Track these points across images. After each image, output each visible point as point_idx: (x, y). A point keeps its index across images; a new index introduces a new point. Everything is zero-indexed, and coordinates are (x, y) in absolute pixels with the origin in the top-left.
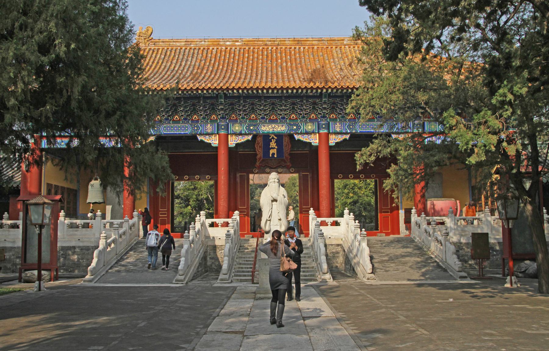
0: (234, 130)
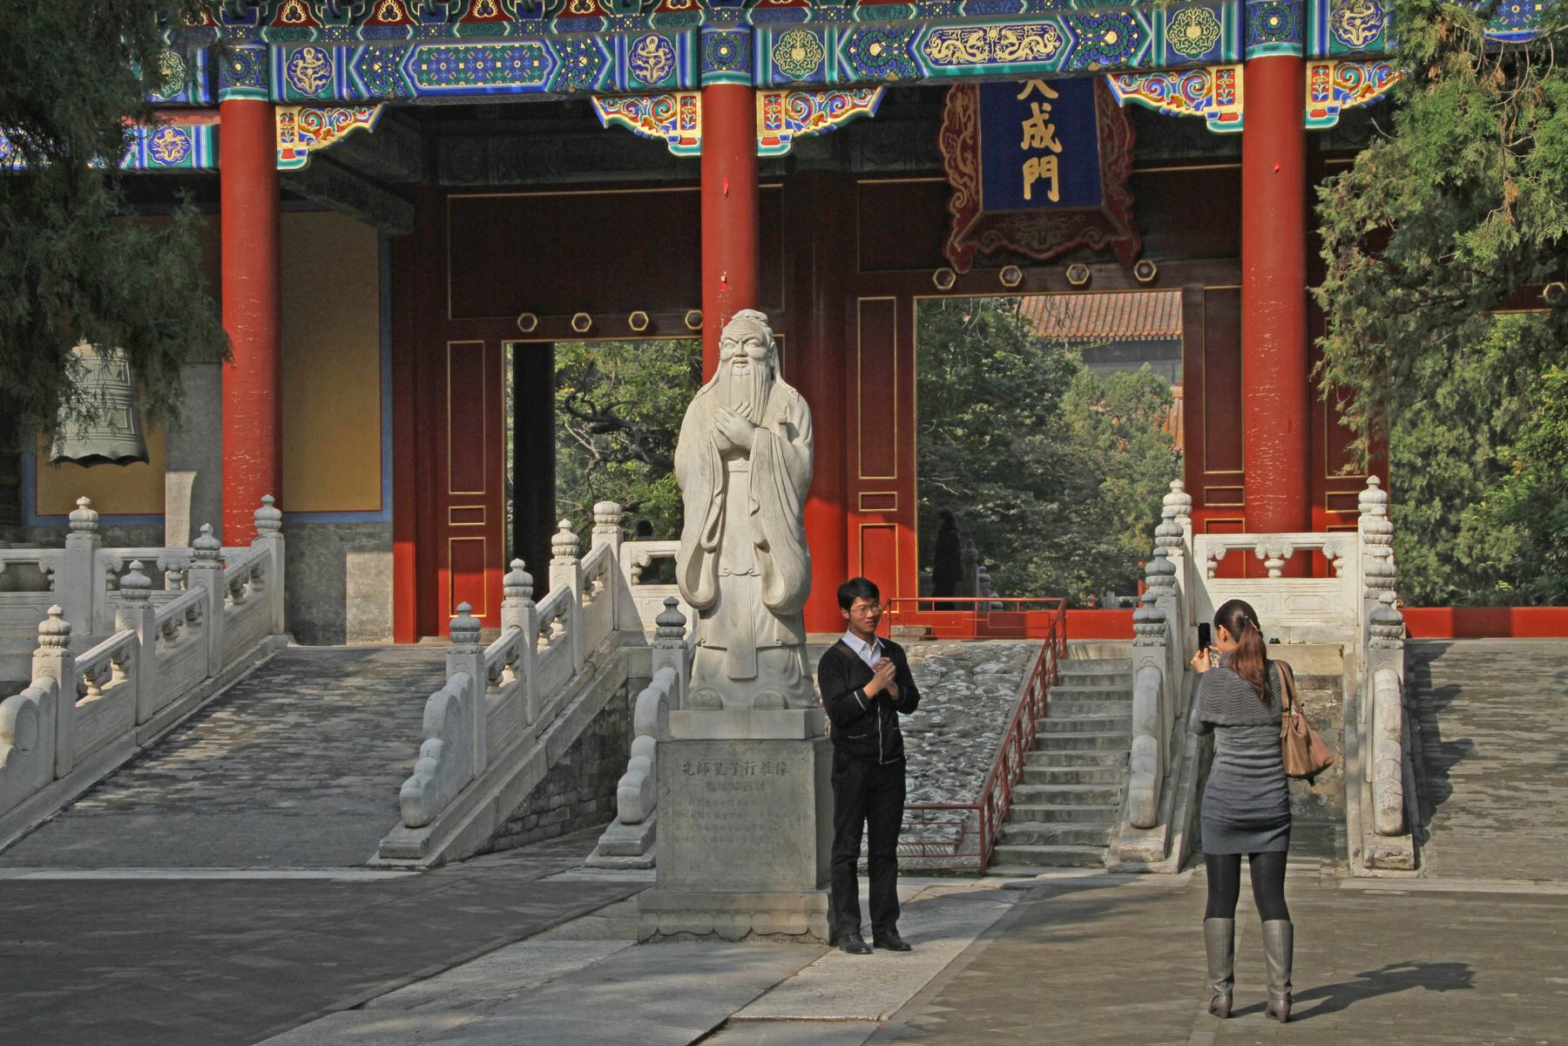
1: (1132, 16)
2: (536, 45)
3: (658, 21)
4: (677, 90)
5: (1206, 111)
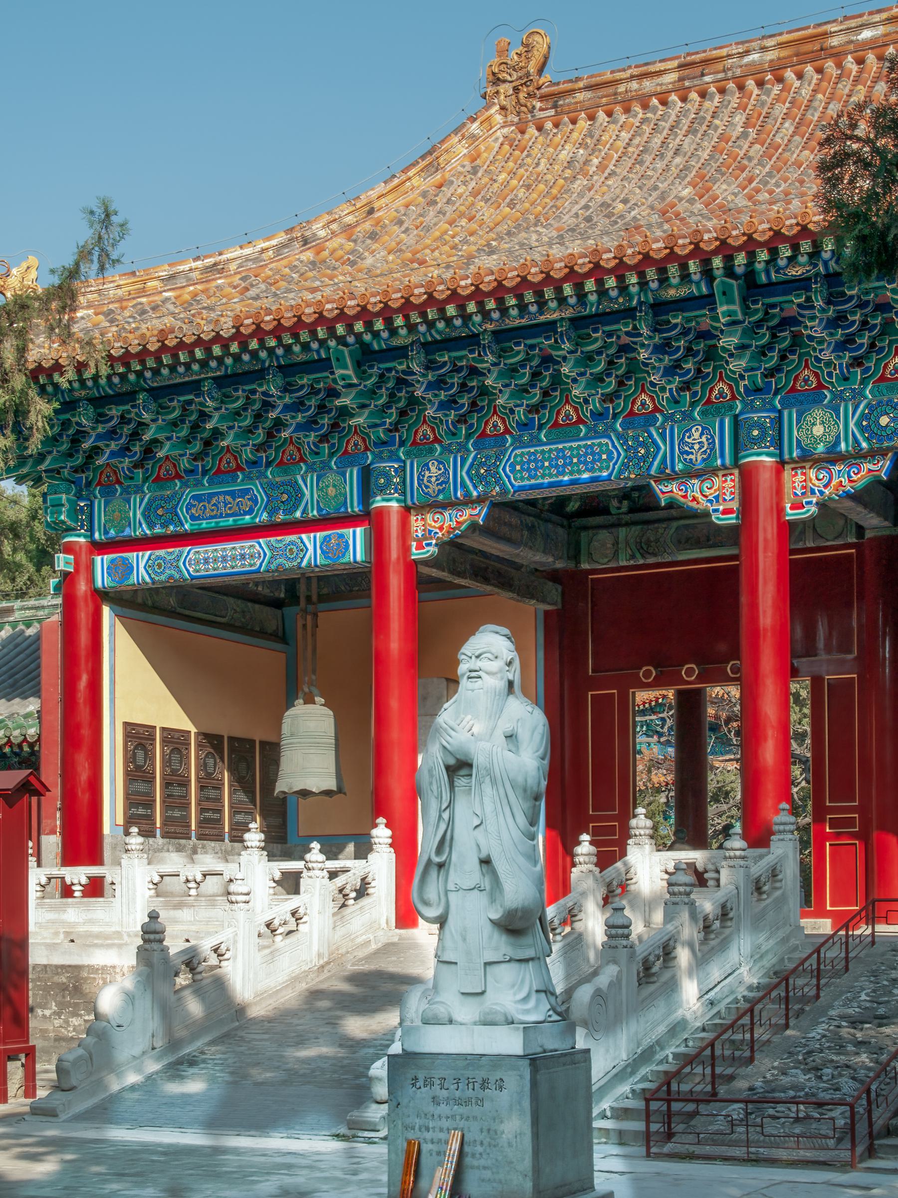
2: (604, 441)
3: (703, 413)
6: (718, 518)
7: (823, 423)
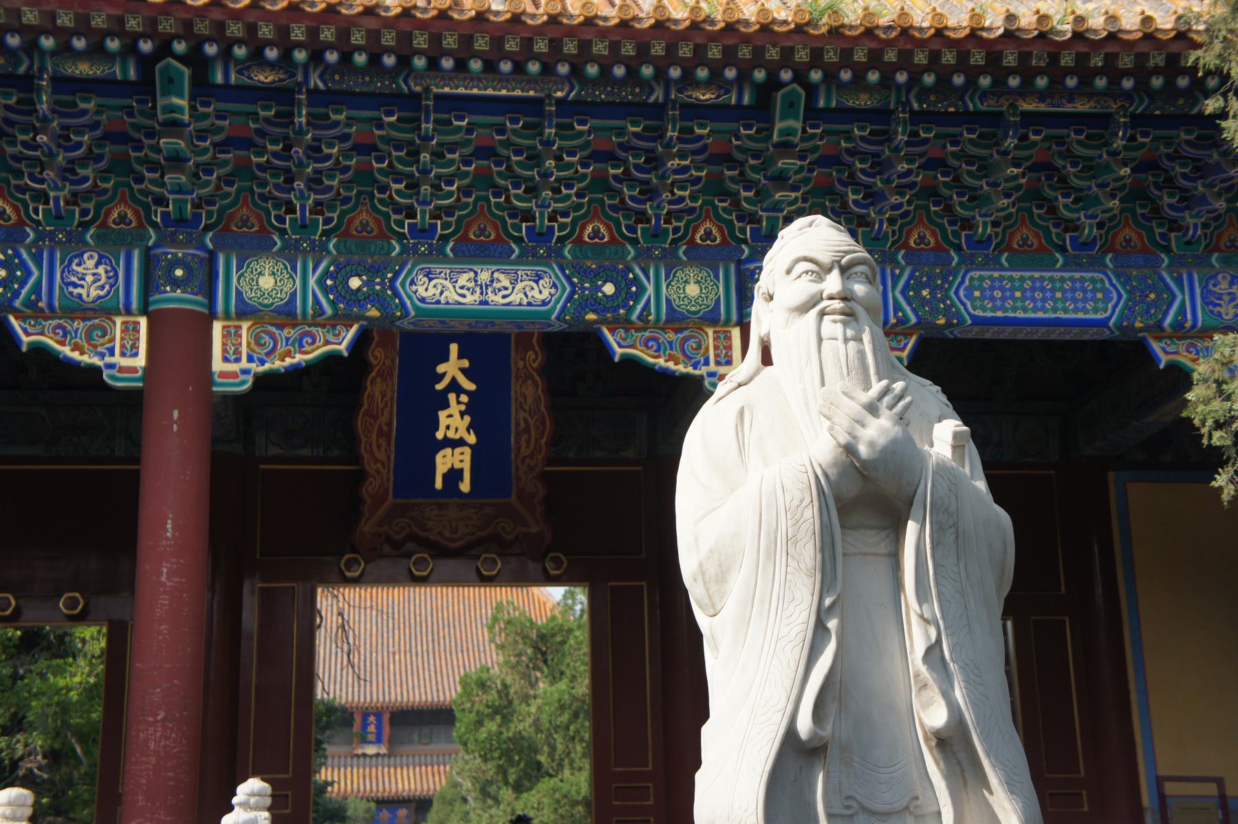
0: (248, 294)
1: (631, 270)
3: (96, 237)
4: (119, 313)
5: (703, 371)
6: (112, 377)
7: (273, 274)
